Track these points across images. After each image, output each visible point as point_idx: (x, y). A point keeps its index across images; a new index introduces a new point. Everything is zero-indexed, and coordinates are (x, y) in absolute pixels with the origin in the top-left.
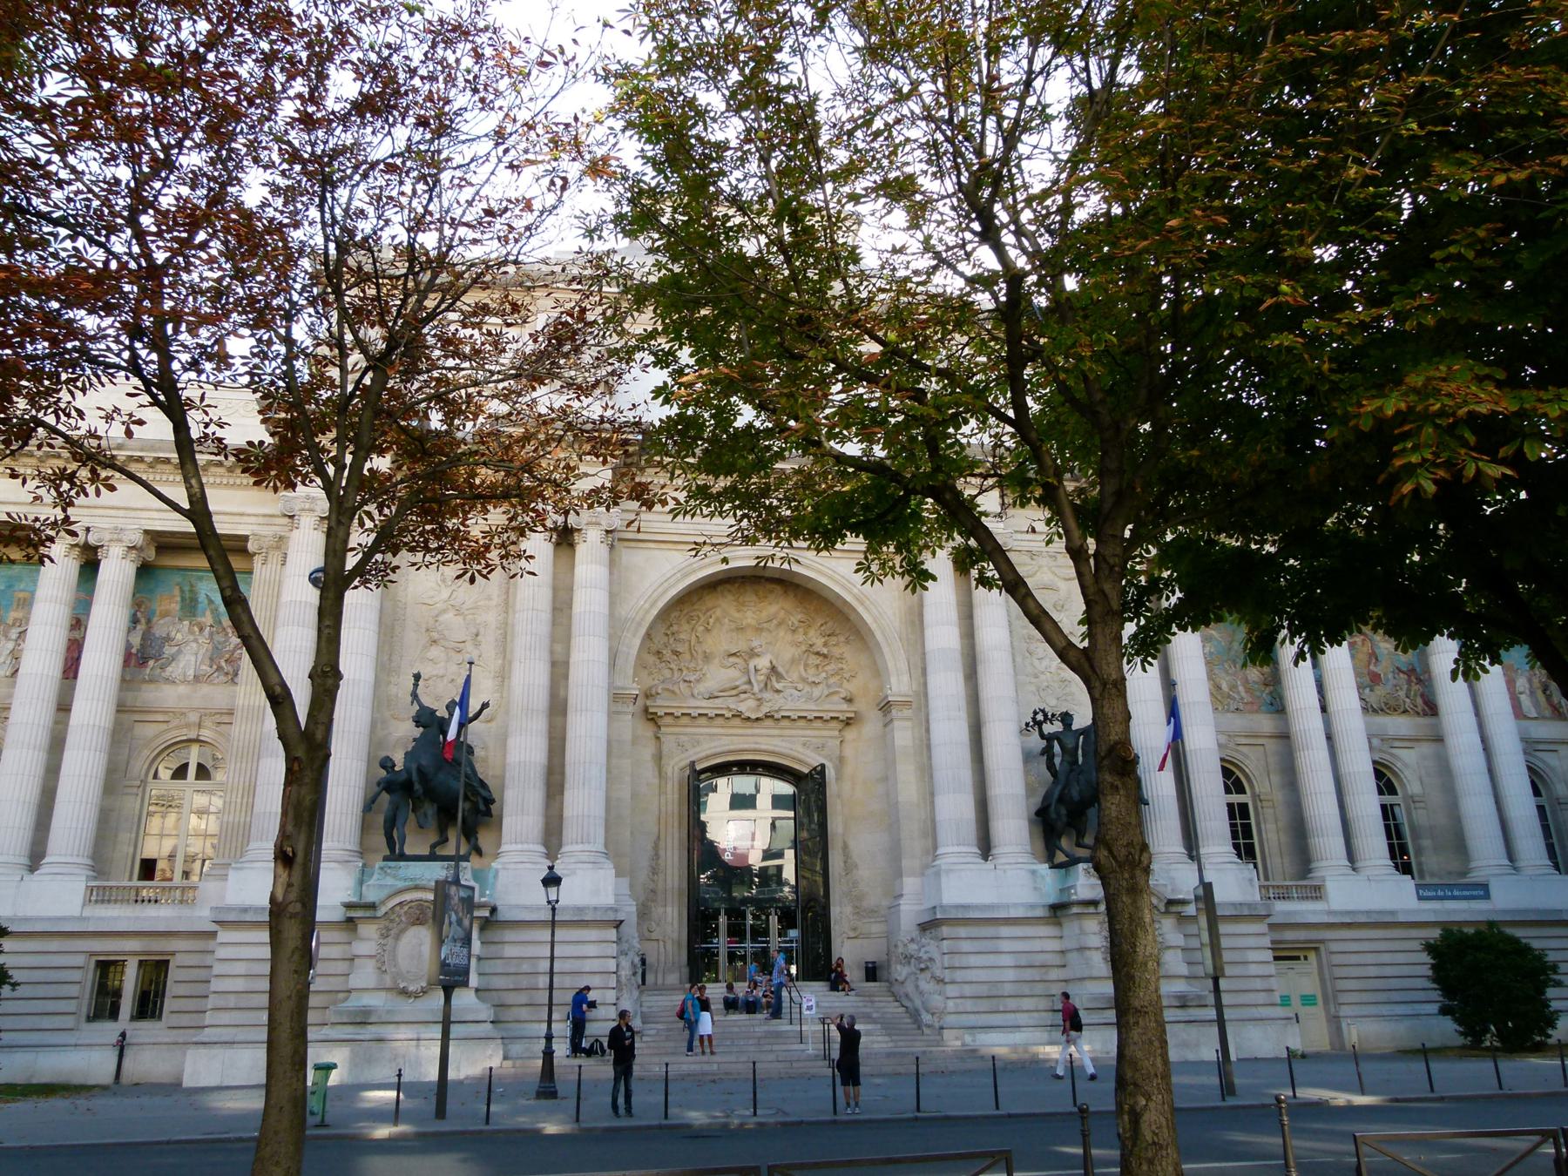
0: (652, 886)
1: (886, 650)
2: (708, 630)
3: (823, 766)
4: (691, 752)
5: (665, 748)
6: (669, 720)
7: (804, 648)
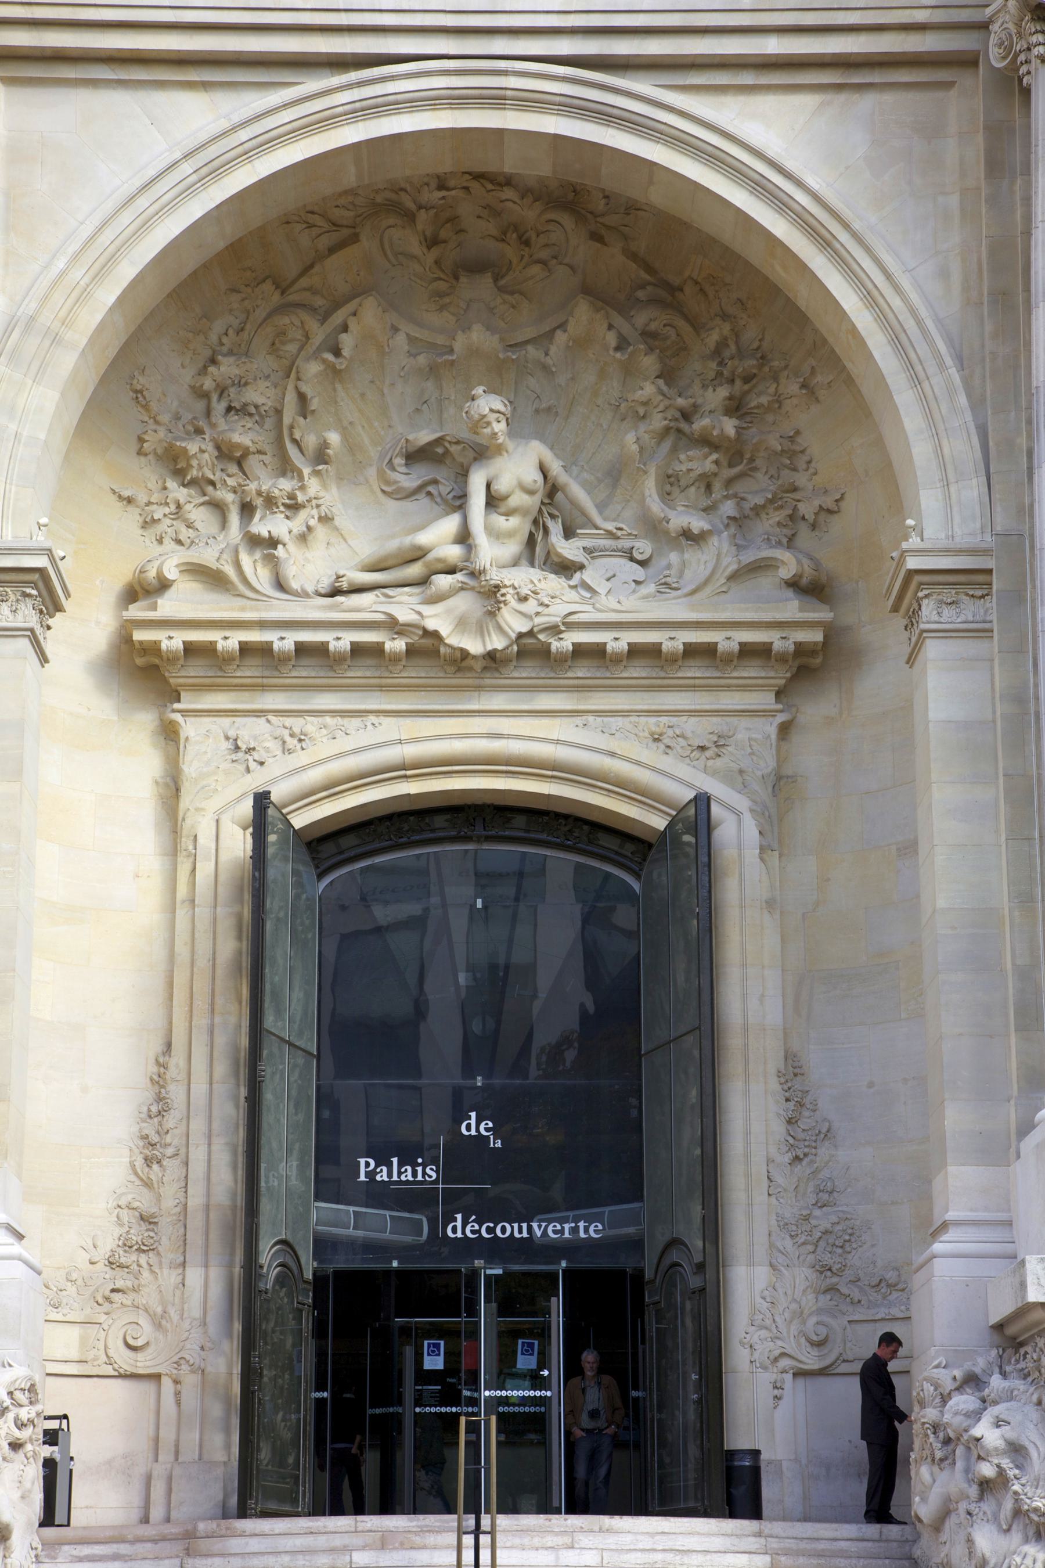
0: (145, 1202)
1: (904, 397)
2: (335, 374)
3: (702, 801)
4: (277, 766)
5: (191, 767)
6: (195, 671)
7: (658, 422)
